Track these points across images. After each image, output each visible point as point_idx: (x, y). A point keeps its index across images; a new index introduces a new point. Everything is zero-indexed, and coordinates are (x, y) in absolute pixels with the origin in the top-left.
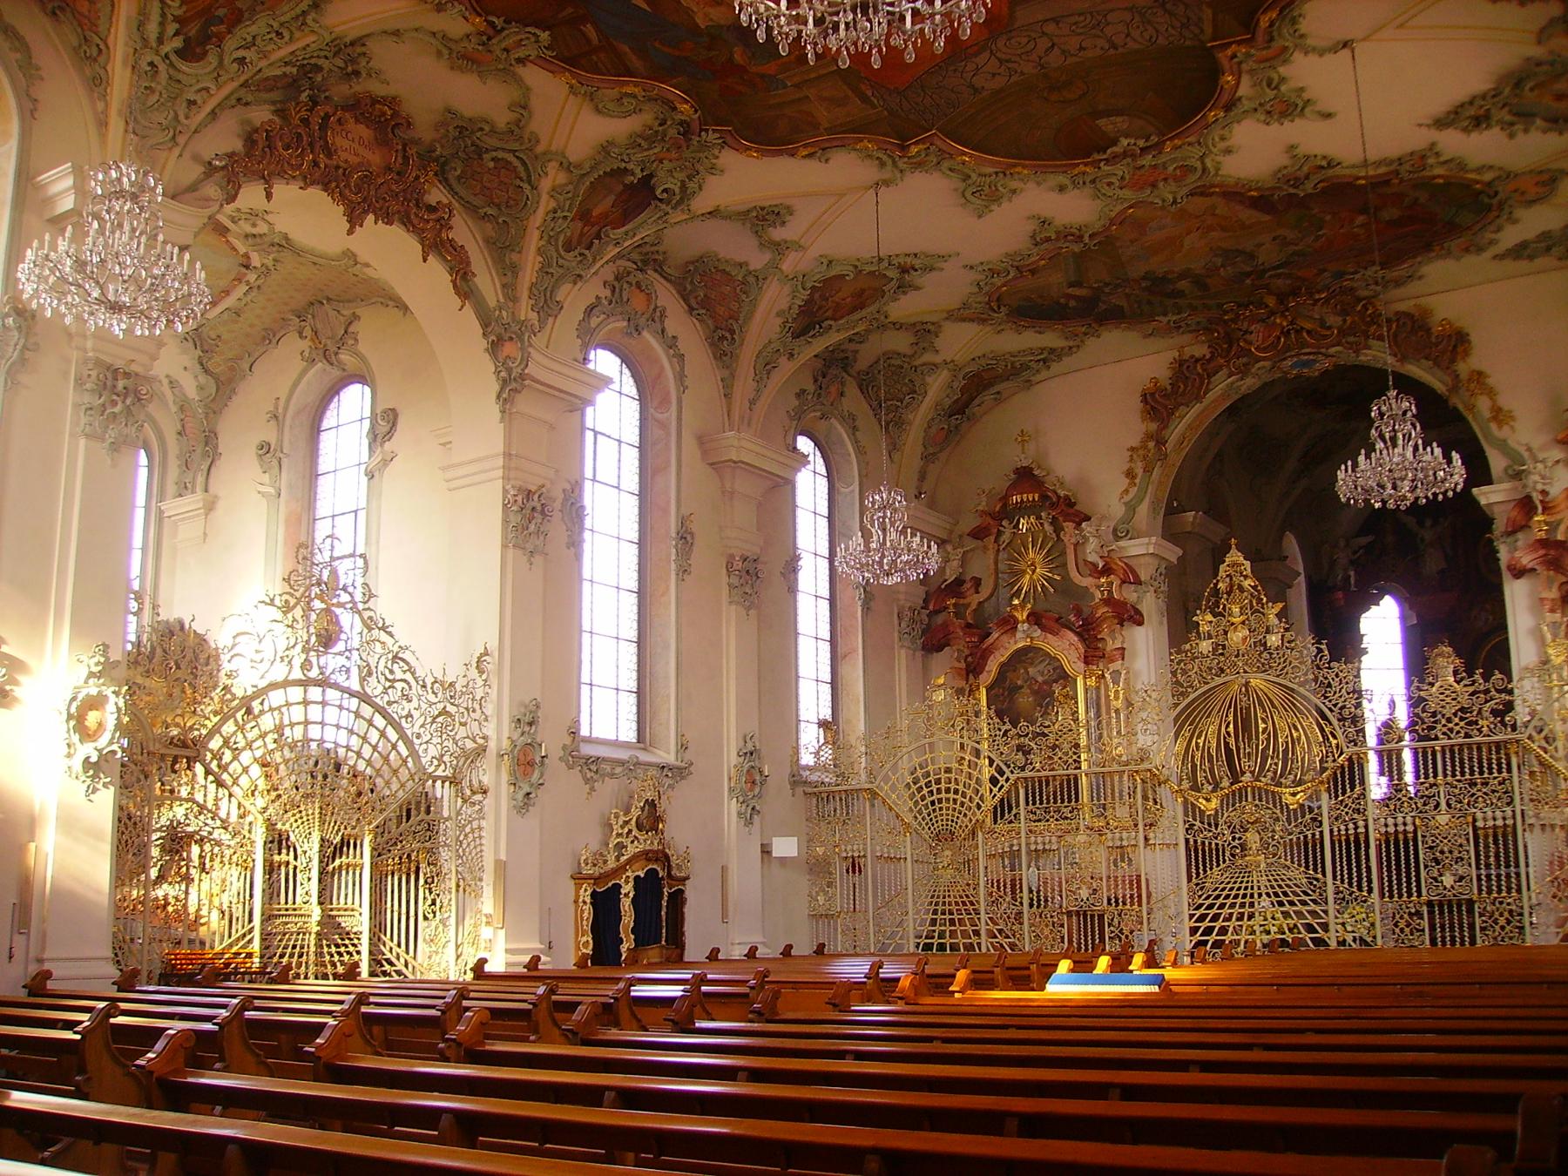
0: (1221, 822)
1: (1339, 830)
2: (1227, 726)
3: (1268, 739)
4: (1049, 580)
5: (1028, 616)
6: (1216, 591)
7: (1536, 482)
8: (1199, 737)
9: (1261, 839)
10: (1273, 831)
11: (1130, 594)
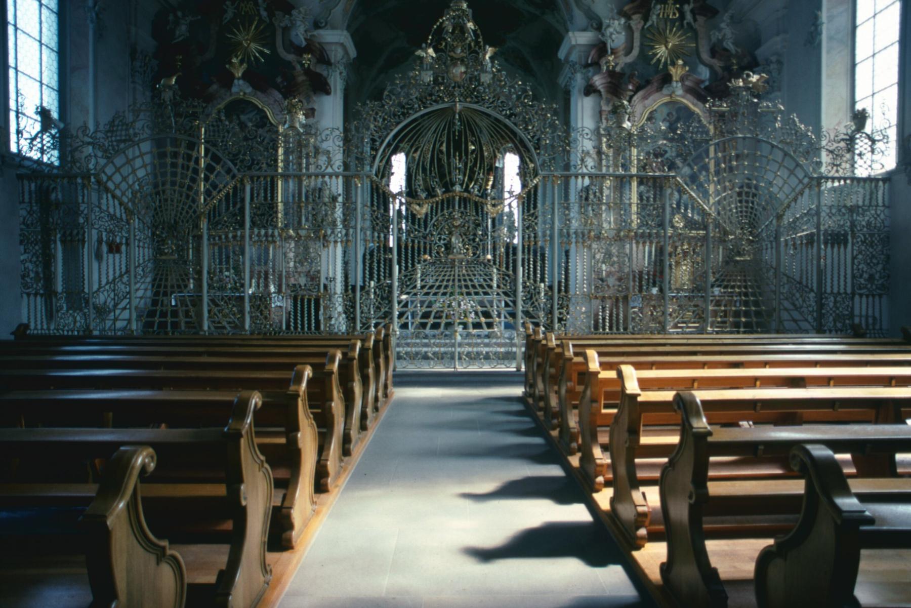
0: (430, 224)
1: (529, 238)
2: (441, 145)
3: (476, 159)
4: (261, 53)
5: (244, 74)
6: (441, 29)
7: (611, 34)
8: (416, 151)
9: (463, 240)
10: (475, 235)
11: (321, 69)
